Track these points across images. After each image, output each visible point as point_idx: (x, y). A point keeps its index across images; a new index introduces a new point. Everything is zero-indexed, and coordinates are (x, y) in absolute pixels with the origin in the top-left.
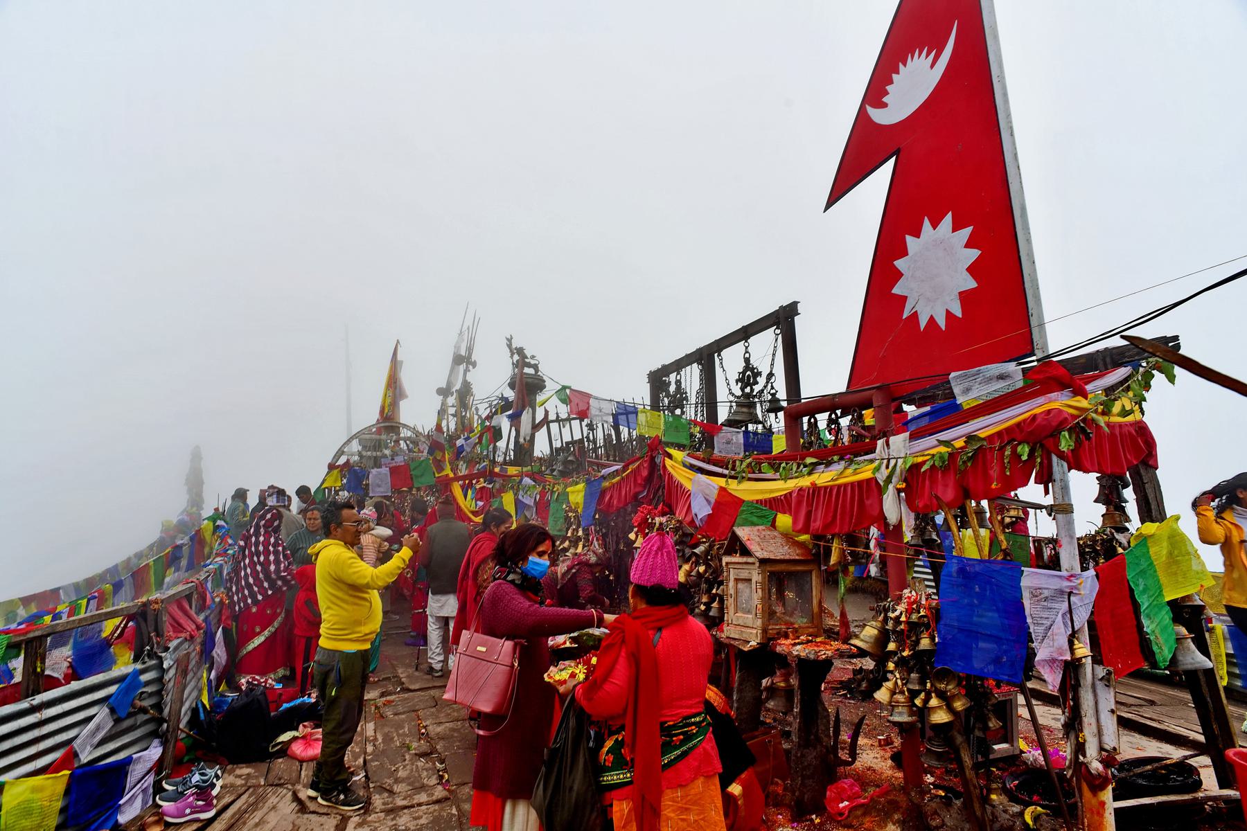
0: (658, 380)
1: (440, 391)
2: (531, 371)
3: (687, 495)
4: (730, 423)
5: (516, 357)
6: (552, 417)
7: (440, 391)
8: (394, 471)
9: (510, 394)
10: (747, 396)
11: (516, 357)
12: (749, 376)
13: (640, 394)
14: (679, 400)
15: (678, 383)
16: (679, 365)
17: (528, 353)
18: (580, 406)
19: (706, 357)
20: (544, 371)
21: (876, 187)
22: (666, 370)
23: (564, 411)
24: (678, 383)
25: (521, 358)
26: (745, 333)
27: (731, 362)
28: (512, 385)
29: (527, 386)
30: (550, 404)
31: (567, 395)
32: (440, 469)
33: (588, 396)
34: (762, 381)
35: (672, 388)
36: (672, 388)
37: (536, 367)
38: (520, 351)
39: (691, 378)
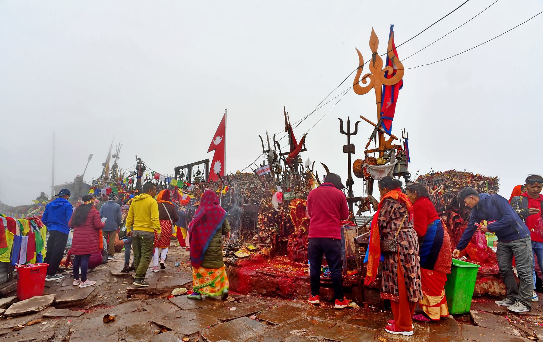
0: (177, 170)
1: (103, 164)
2: (142, 165)
3: (182, 197)
4: (193, 184)
5: (138, 161)
6: (148, 178)
7: (103, 164)
8: (107, 190)
9: (136, 171)
10: (198, 178)
11: (138, 161)
12: (199, 173)
13: (172, 174)
14: (182, 176)
15: (182, 172)
16: (183, 167)
17: (142, 160)
18: (157, 176)
19: (190, 167)
20: (146, 165)
21: (214, 151)
22: (180, 168)
23: (152, 177)
24: (182, 172)
25: (140, 161)
26: (198, 163)
27: (195, 169)
28: (137, 169)
29: (141, 169)
30: (147, 174)
31: (153, 173)
32: (119, 190)
33: (160, 174)
34: (201, 174)
35: (181, 173)
36: (181, 173)
37: (144, 164)
38: (140, 159)
39: (186, 171)
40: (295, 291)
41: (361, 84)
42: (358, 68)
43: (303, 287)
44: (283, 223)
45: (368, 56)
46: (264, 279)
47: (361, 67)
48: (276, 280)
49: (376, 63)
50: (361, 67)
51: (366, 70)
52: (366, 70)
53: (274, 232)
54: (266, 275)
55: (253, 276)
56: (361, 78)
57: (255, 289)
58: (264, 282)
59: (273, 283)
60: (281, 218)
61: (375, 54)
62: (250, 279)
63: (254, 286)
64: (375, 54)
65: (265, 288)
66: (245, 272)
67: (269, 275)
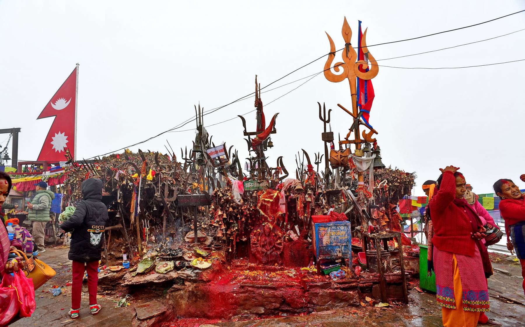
40: (310, 302)
41: (332, 71)
42: (330, 54)
43: (322, 295)
44: (243, 219)
45: (340, 44)
46: (259, 294)
47: (332, 54)
48: (278, 293)
49: (349, 55)
50: (332, 54)
51: (339, 58)
52: (339, 58)
53: (234, 231)
54: (261, 288)
55: (237, 293)
56: (332, 65)
57: (244, 309)
58: (260, 298)
59: (275, 296)
60: (242, 213)
61: (348, 45)
62: (233, 298)
63: (241, 305)
64: (348, 45)
65: (262, 305)
66: (216, 288)
67: (265, 288)
